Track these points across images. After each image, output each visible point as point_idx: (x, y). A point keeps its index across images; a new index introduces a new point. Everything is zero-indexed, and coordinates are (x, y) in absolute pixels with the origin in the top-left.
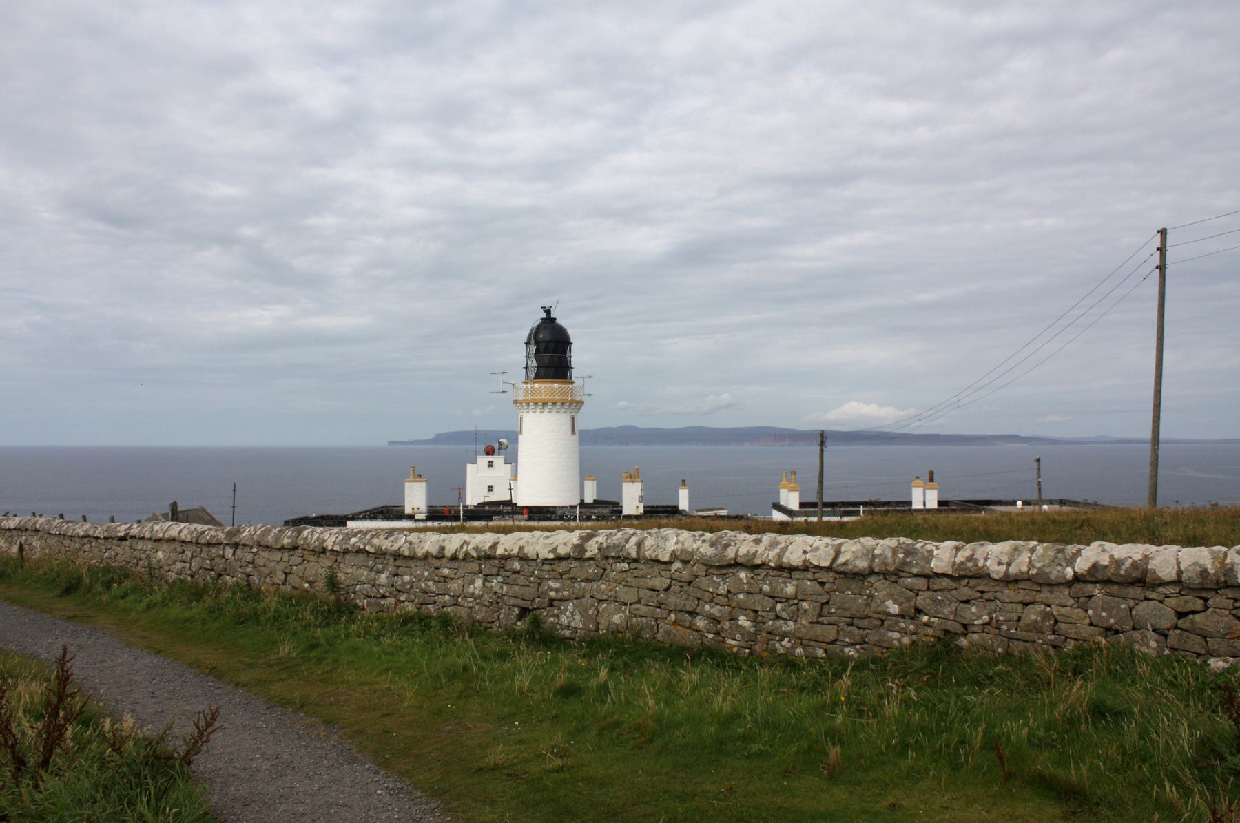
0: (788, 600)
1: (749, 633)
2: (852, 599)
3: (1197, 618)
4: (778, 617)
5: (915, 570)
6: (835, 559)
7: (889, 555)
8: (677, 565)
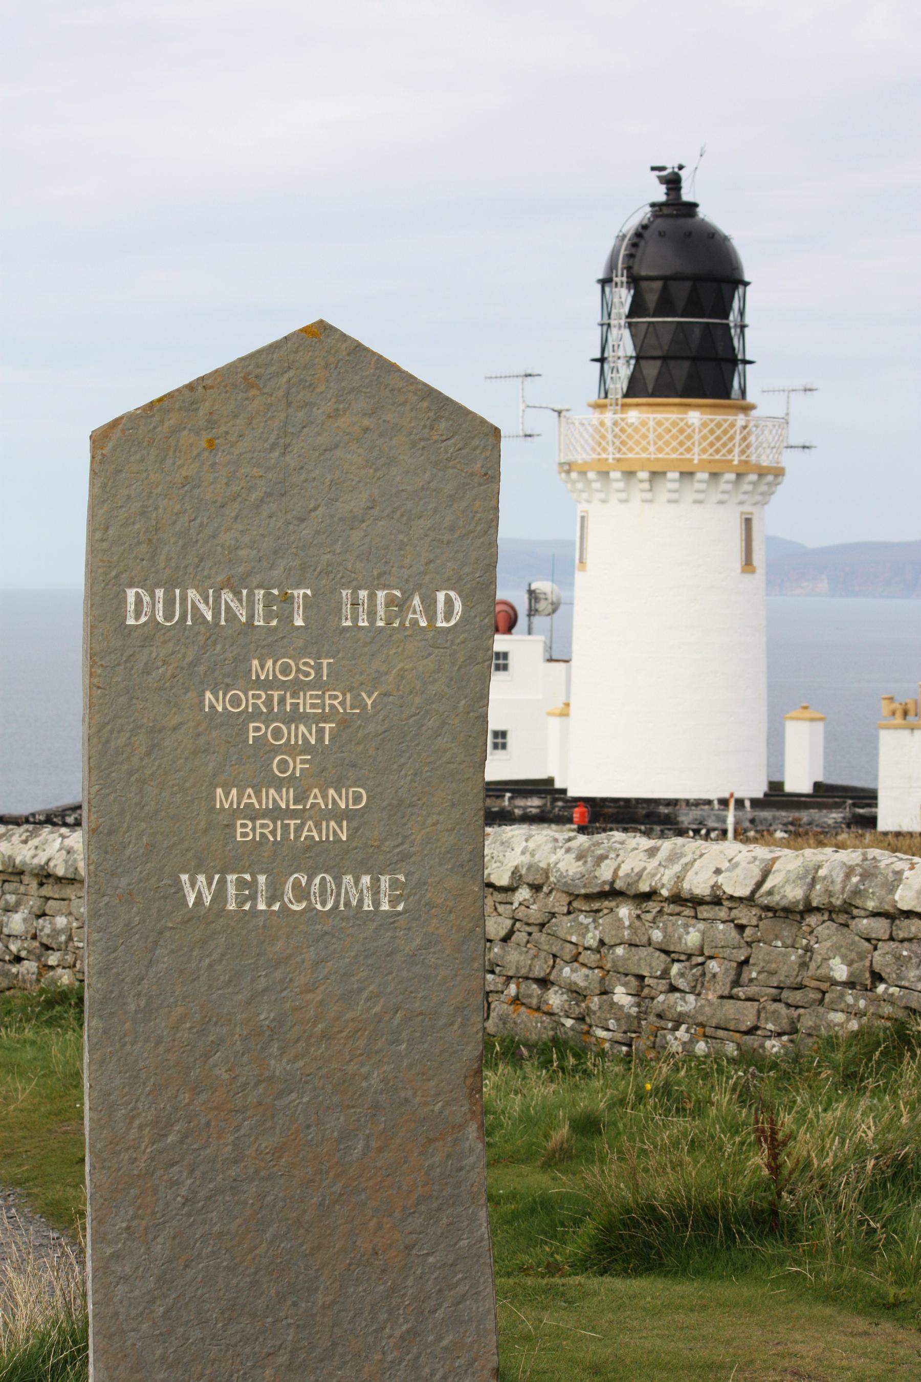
0: (690, 956)
1: (629, 1016)
2: (778, 955)
4: (673, 989)
5: (871, 905)
6: (759, 884)
7: (839, 877)
8: (524, 893)
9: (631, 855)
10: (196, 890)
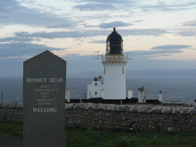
3: (167, 120)
6: (115, 109)
8: (90, 110)
9: (101, 106)
10: (35, 110)
